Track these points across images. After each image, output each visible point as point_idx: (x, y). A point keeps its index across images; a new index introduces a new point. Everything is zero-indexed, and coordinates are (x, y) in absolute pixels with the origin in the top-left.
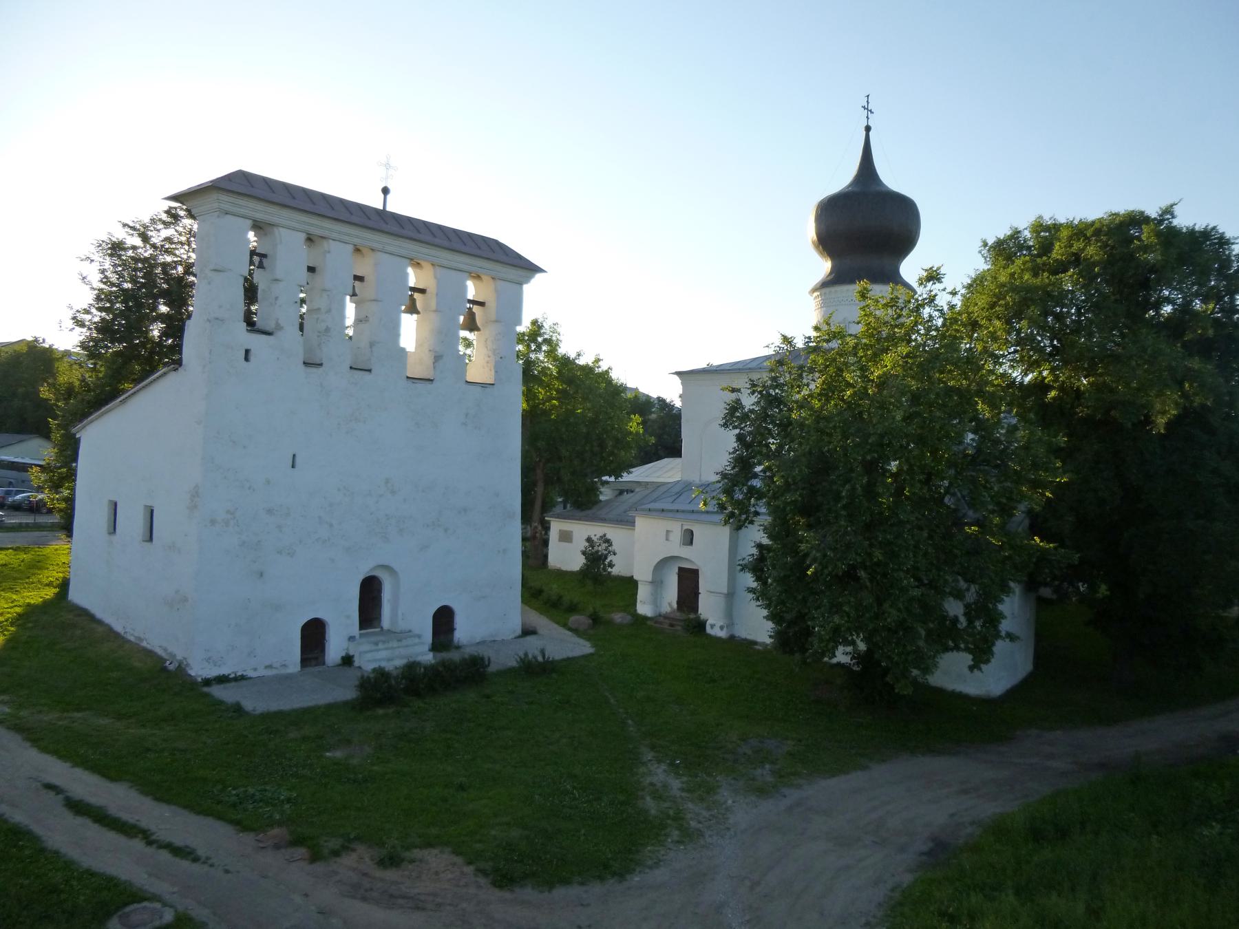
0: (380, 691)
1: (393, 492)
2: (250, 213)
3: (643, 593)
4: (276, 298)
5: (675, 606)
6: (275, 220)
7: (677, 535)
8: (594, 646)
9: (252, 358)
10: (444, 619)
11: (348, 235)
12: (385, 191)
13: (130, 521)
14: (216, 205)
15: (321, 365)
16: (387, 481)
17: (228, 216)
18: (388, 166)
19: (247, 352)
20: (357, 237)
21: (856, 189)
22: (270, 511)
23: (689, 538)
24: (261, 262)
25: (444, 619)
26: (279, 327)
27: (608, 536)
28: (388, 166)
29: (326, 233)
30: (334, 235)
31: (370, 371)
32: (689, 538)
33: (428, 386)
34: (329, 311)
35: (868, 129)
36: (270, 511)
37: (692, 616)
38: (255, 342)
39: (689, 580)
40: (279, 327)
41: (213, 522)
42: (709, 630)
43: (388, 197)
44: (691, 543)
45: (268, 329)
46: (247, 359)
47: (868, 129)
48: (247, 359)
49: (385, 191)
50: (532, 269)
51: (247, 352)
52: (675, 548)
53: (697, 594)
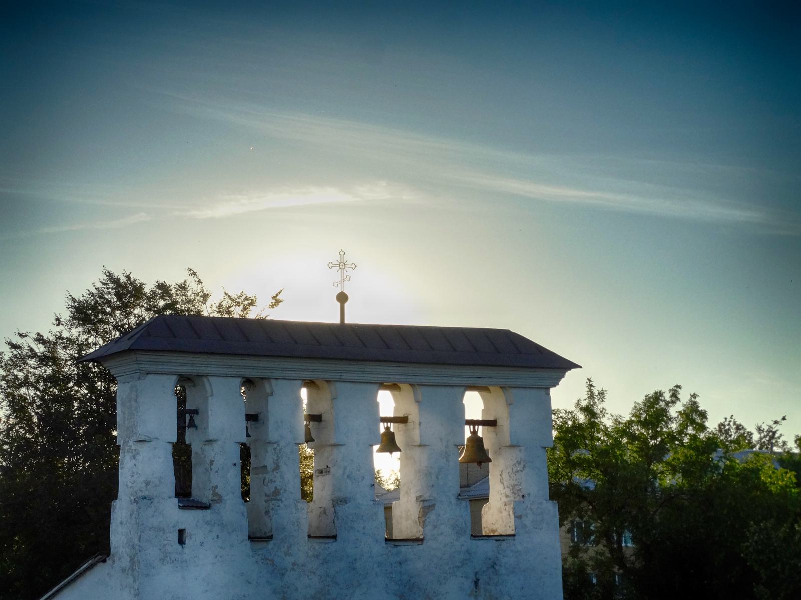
2: (172, 368)
4: (212, 462)
6: (203, 370)
11: (293, 370)
12: (342, 298)
14: (136, 366)
15: (271, 537)
17: (150, 376)
18: (342, 265)
19: (181, 532)
20: (305, 370)
24: (192, 420)
26: (219, 499)
30: (278, 374)
31: (334, 537)
34: (277, 467)
38: (189, 519)
40: (219, 499)
43: (346, 305)
46: (181, 541)
48: (181, 541)
49: (342, 298)
51: (181, 532)
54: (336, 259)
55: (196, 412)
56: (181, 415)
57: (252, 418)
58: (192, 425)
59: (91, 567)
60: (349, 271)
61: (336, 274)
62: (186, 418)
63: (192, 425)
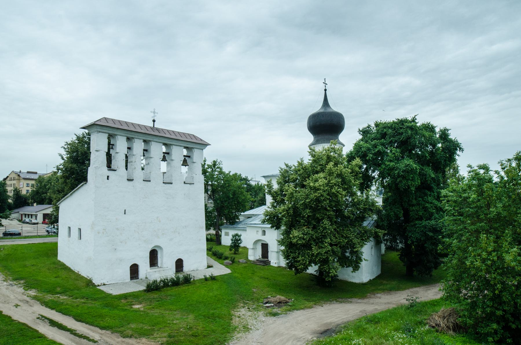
0: (153, 288)
1: (160, 221)
3: (250, 252)
5: (261, 257)
7: (260, 232)
8: (231, 270)
9: (110, 178)
10: (179, 264)
12: (154, 121)
13: (75, 233)
16: (157, 217)
18: (154, 112)
19: (108, 177)
21: (322, 111)
22: (117, 229)
23: (264, 233)
25: (179, 264)
27: (239, 234)
28: (154, 112)
29: (133, 136)
30: (136, 137)
32: (264, 233)
33: (170, 185)
35: (325, 90)
36: (117, 229)
37: (266, 260)
38: (110, 173)
39: (265, 247)
41: (99, 233)
42: (271, 264)
44: (265, 235)
45: (115, 169)
46: (108, 179)
47: (325, 90)
48: (108, 179)
49: (154, 121)
50: (206, 145)
51: (108, 177)
52: (259, 236)
53: (268, 252)
54: (153, 110)
55: (113, 145)
56: (109, 144)
57: (129, 148)
58: (112, 148)
59: (82, 185)
60: (156, 114)
61: (152, 114)
62: (110, 146)
63: (112, 148)
